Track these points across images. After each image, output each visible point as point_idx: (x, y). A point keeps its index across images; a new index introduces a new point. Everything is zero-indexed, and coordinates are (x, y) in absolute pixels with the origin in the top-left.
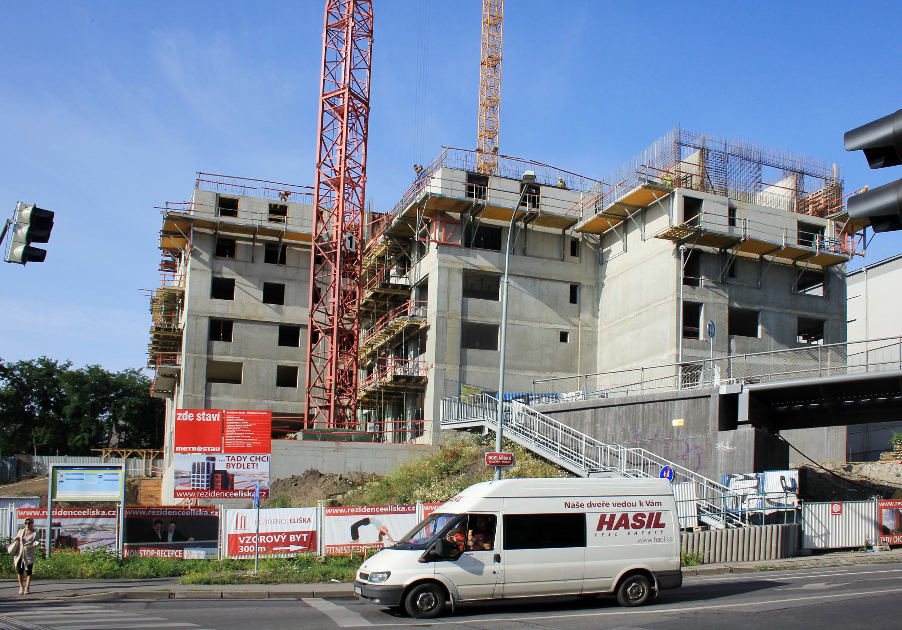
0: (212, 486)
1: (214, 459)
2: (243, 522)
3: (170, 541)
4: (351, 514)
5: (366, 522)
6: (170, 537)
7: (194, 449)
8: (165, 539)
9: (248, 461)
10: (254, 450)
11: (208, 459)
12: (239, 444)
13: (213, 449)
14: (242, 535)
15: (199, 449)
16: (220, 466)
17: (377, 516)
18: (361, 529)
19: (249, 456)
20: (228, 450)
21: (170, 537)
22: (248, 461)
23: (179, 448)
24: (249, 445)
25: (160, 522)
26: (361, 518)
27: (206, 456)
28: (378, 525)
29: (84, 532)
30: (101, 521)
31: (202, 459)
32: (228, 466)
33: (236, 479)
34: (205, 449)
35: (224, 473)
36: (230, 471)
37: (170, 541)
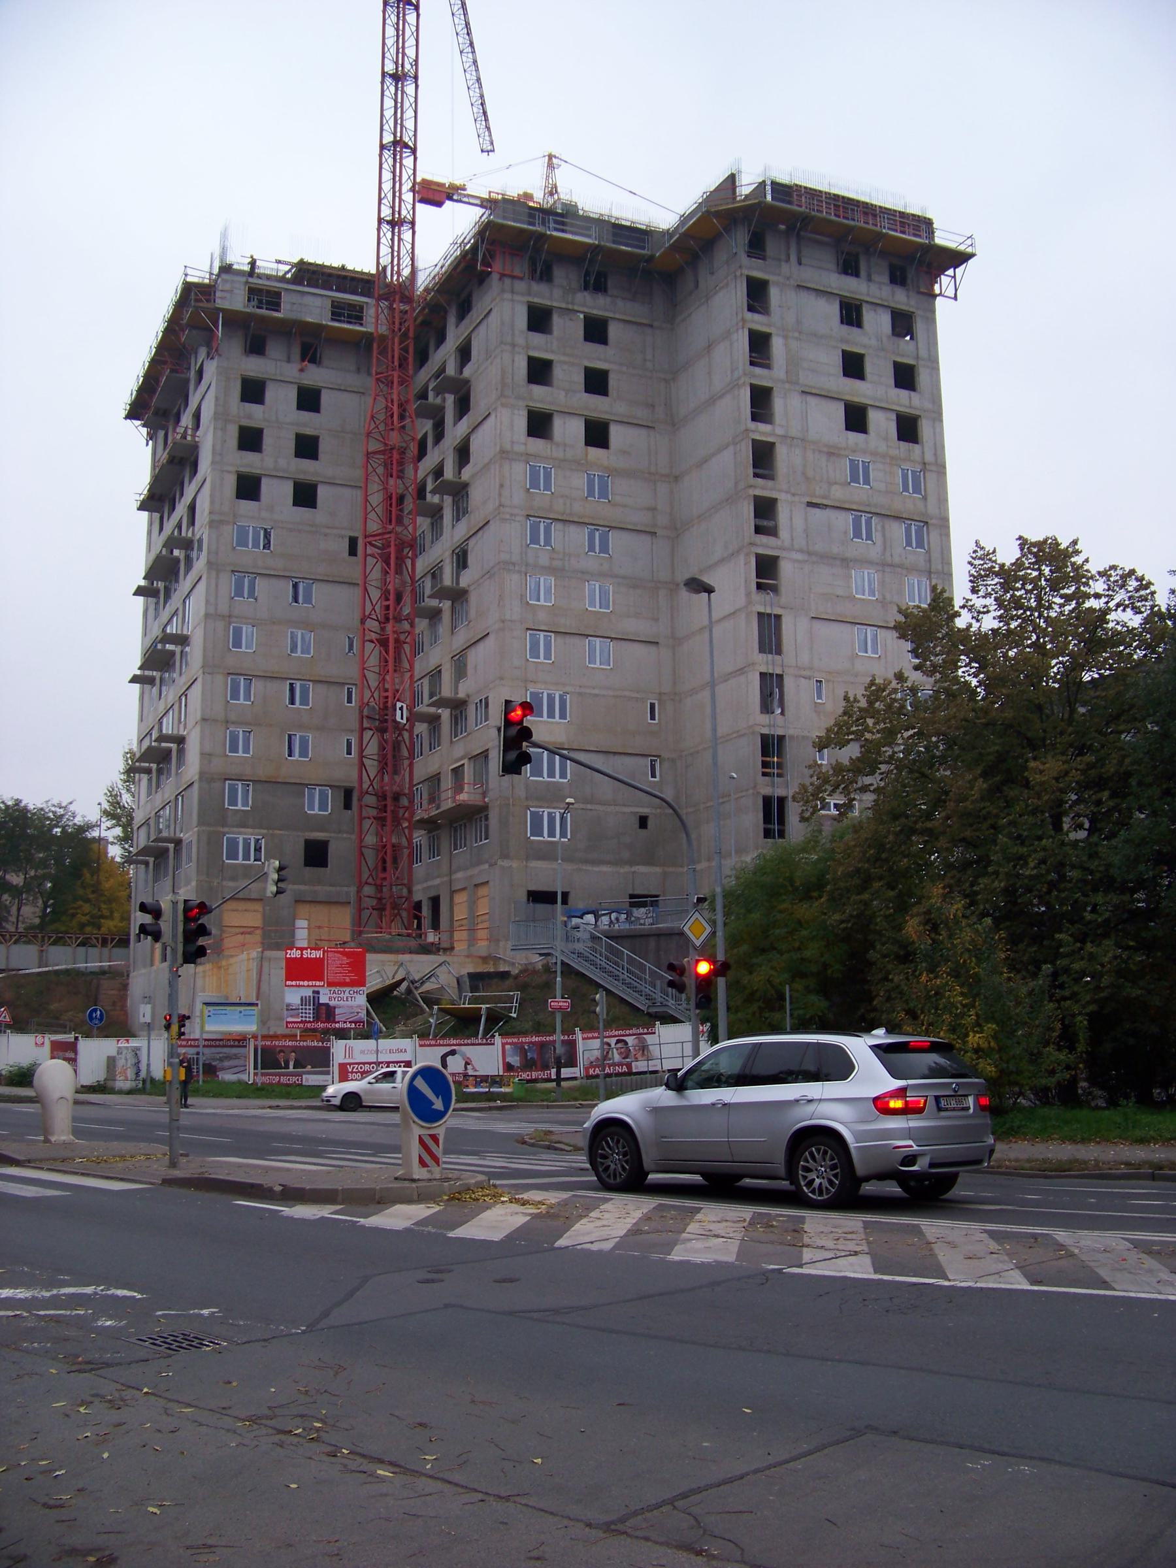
0: (317, 1018)
1: (318, 993)
2: (349, 1051)
3: (291, 1069)
4: (440, 1045)
5: (453, 1053)
6: (291, 1064)
7: (301, 983)
8: (287, 1067)
9: (347, 994)
10: (352, 984)
11: (314, 992)
12: (339, 978)
13: (318, 983)
14: (350, 1064)
15: (306, 983)
16: (323, 1000)
17: (463, 1048)
18: (449, 1059)
19: (347, 989)
20: (330, 984)
21: (291, 1064)
22: (347, 994)
23: (289, 983)
24: (348, 980)
25: (281, 1051)
26: (448, 1049)
27: (312, 989)
28: (464, 1056)
29: (221, 1060)
30: (234, 1051)
31: (308, 992)
32: (330, 999)
33: (337, 1011)
34: (310, 983)
35: (327, 1005)
36: (332, 1003)
37: (291, 1069)
